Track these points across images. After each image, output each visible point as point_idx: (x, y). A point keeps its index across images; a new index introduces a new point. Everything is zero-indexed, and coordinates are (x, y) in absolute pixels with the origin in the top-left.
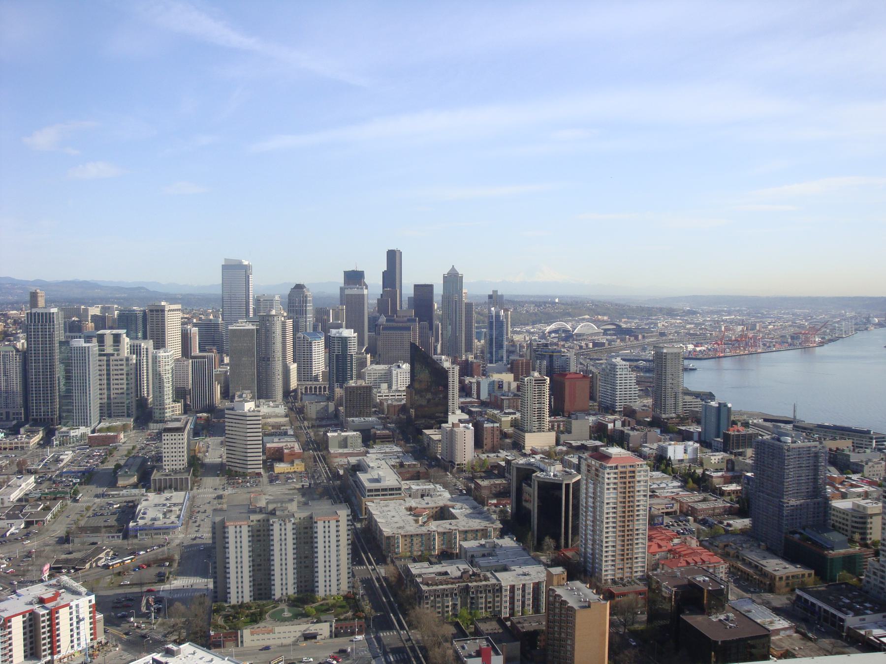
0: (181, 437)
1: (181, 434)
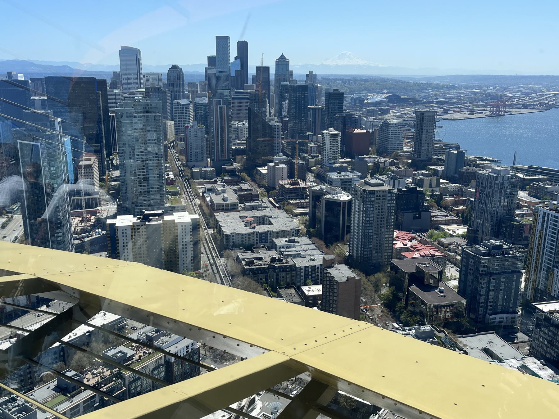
0: (91, 171)
1: (91, 169)
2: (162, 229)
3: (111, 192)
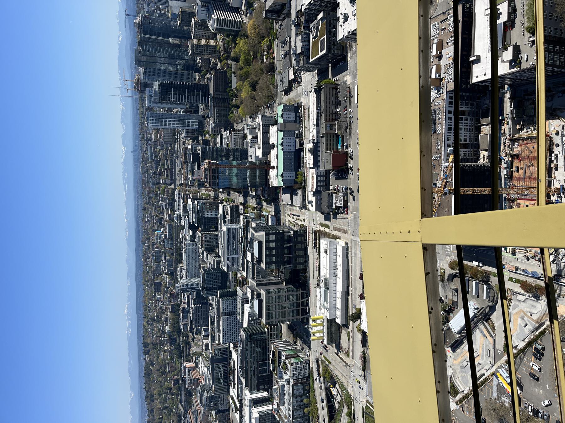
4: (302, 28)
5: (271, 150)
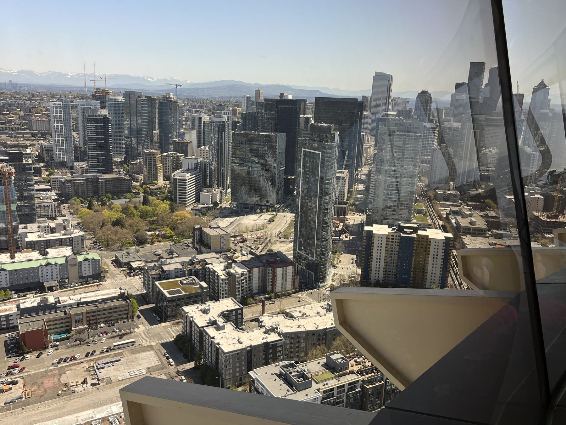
2: (415, 242)
3: (357, 203)
4: (190, 267)
5: (38, 252)
